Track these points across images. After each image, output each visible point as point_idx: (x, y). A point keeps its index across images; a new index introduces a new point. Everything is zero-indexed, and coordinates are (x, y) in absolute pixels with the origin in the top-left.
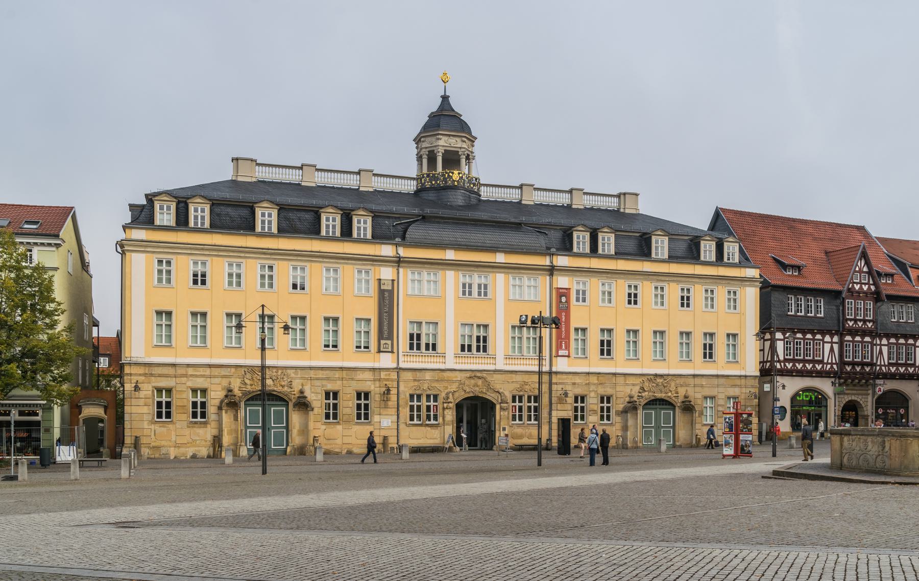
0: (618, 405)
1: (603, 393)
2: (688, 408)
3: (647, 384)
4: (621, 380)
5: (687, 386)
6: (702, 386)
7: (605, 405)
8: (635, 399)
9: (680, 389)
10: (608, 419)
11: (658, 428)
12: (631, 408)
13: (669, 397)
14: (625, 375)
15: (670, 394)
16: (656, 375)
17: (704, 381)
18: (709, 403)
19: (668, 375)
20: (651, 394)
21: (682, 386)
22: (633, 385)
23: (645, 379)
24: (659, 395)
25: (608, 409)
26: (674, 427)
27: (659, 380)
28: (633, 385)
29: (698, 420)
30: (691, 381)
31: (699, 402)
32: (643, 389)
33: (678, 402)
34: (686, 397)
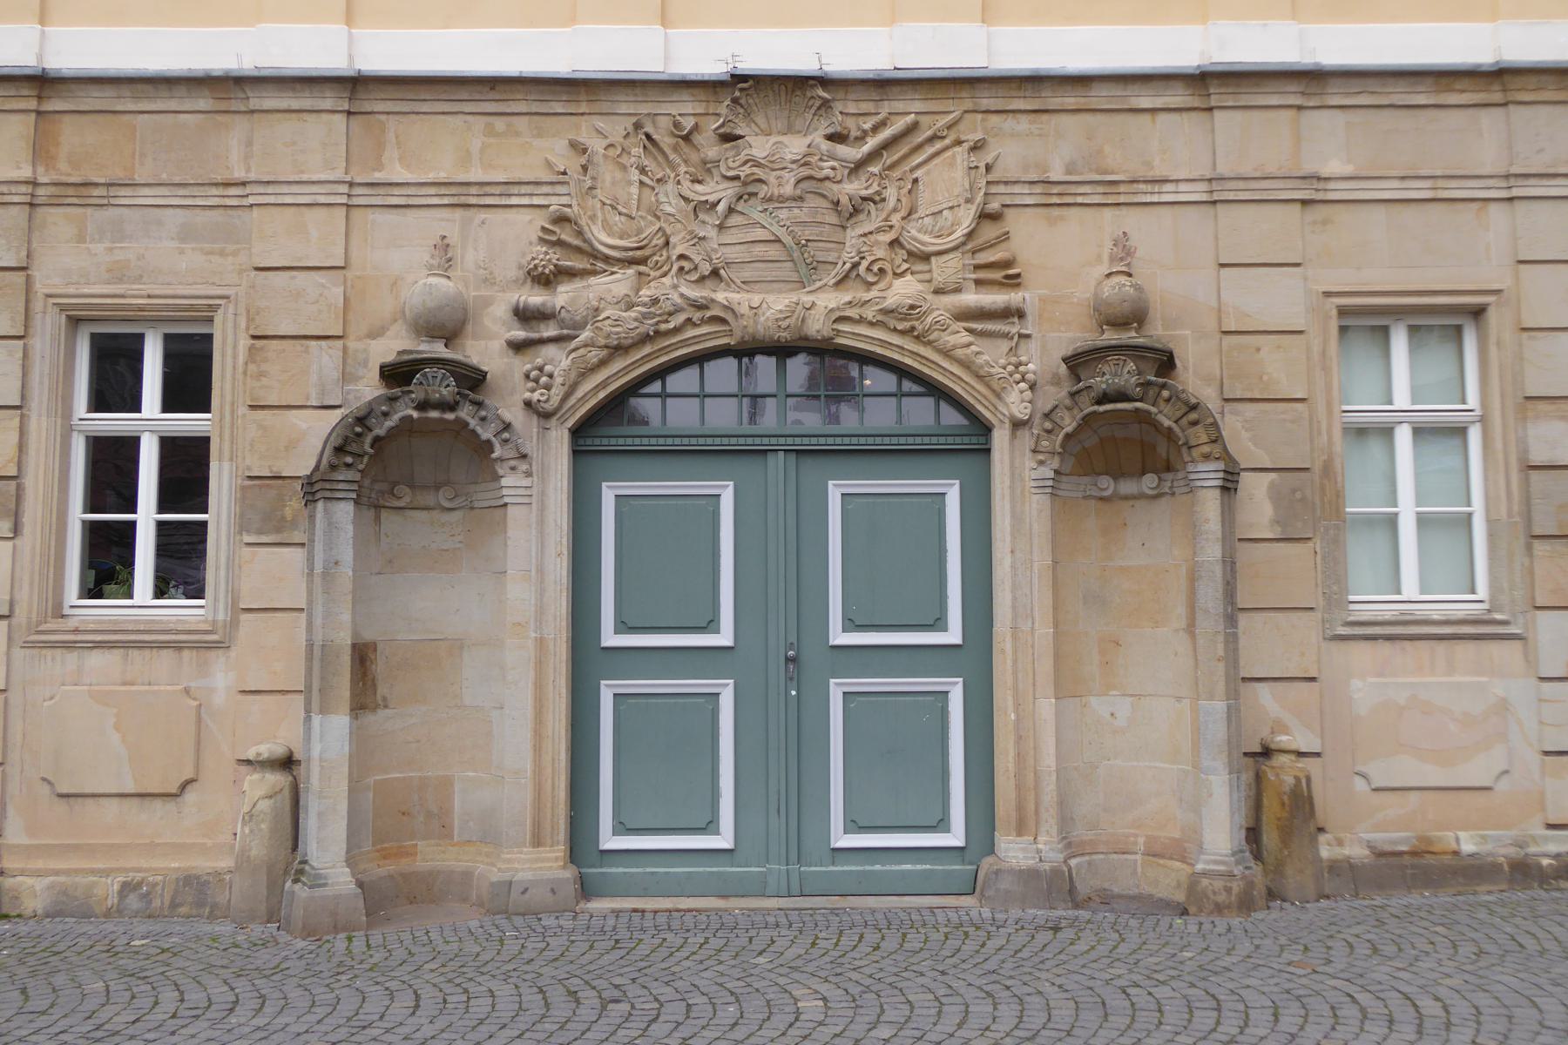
0: (269, 426)
1: (96, 289)
2: (1131, 423)
3: (619, 184)
4: (315, 145)
5: (1117, 192)
6: (1312, 196)
7: (151, 420)
8: (486, 349)
9: (1031, 238)
10: (182, 562)
11: (787, 666)
12: (414, 441)
13: (905, 319)
14: (355, 85)
15: (903, 290)
16: (745, 88)
17: (1331, 144)
18: (1403, 378)
19: (882, 85)
20: (671, 289)
21: (1056, 197)
22: (463, 197)
23: (602, 130)
24: (767, 306)
25: (186, 470)
26: (974, 661)
27: (779, 145)
28: (463, 197)
29: (1286, 571)
30: (1175, 145)
31: (1280, 368)
32: (569, 254)
33: (1019, 380)
34: (1135, 317)
